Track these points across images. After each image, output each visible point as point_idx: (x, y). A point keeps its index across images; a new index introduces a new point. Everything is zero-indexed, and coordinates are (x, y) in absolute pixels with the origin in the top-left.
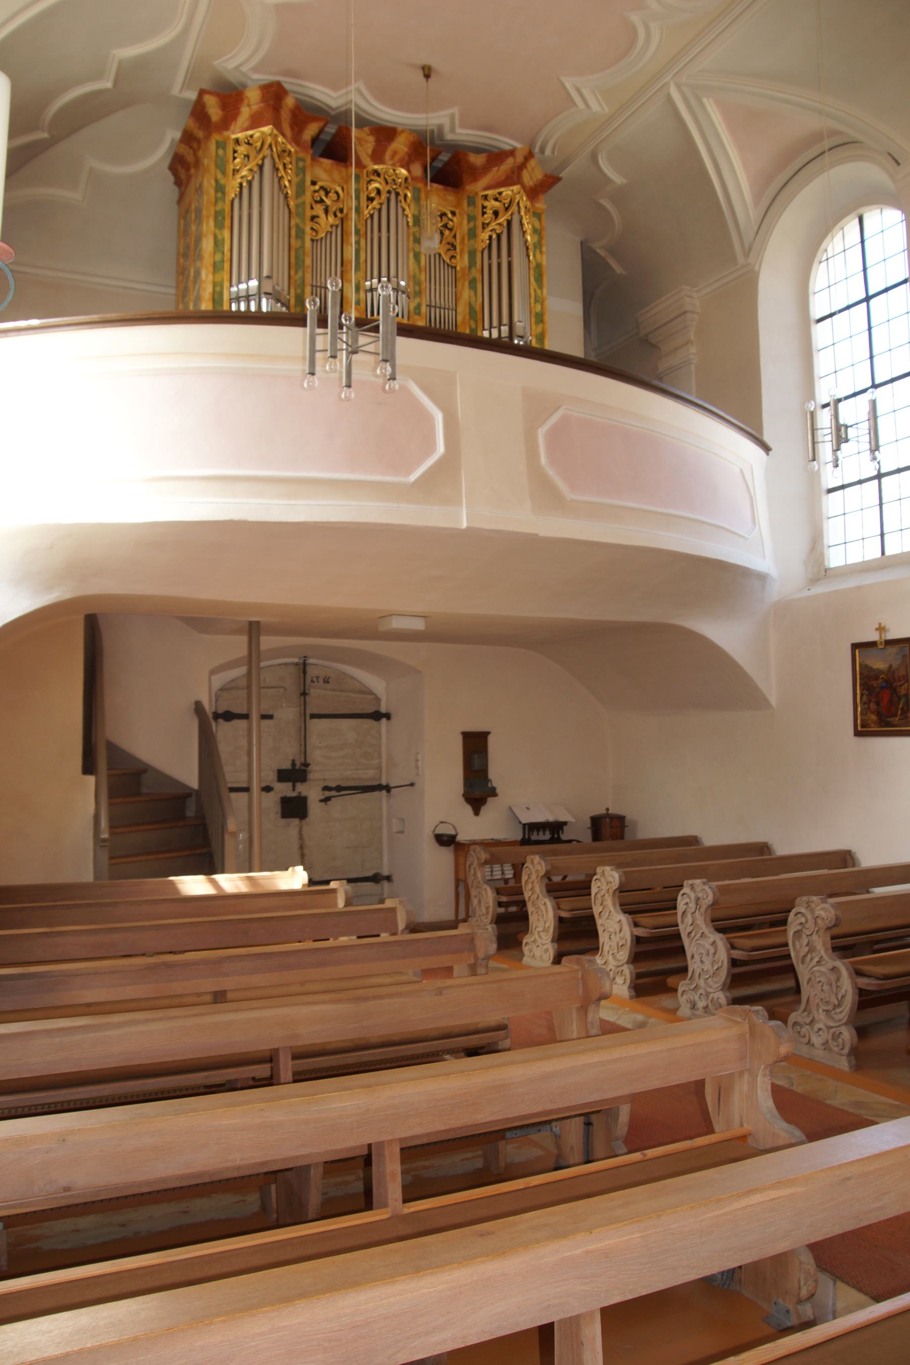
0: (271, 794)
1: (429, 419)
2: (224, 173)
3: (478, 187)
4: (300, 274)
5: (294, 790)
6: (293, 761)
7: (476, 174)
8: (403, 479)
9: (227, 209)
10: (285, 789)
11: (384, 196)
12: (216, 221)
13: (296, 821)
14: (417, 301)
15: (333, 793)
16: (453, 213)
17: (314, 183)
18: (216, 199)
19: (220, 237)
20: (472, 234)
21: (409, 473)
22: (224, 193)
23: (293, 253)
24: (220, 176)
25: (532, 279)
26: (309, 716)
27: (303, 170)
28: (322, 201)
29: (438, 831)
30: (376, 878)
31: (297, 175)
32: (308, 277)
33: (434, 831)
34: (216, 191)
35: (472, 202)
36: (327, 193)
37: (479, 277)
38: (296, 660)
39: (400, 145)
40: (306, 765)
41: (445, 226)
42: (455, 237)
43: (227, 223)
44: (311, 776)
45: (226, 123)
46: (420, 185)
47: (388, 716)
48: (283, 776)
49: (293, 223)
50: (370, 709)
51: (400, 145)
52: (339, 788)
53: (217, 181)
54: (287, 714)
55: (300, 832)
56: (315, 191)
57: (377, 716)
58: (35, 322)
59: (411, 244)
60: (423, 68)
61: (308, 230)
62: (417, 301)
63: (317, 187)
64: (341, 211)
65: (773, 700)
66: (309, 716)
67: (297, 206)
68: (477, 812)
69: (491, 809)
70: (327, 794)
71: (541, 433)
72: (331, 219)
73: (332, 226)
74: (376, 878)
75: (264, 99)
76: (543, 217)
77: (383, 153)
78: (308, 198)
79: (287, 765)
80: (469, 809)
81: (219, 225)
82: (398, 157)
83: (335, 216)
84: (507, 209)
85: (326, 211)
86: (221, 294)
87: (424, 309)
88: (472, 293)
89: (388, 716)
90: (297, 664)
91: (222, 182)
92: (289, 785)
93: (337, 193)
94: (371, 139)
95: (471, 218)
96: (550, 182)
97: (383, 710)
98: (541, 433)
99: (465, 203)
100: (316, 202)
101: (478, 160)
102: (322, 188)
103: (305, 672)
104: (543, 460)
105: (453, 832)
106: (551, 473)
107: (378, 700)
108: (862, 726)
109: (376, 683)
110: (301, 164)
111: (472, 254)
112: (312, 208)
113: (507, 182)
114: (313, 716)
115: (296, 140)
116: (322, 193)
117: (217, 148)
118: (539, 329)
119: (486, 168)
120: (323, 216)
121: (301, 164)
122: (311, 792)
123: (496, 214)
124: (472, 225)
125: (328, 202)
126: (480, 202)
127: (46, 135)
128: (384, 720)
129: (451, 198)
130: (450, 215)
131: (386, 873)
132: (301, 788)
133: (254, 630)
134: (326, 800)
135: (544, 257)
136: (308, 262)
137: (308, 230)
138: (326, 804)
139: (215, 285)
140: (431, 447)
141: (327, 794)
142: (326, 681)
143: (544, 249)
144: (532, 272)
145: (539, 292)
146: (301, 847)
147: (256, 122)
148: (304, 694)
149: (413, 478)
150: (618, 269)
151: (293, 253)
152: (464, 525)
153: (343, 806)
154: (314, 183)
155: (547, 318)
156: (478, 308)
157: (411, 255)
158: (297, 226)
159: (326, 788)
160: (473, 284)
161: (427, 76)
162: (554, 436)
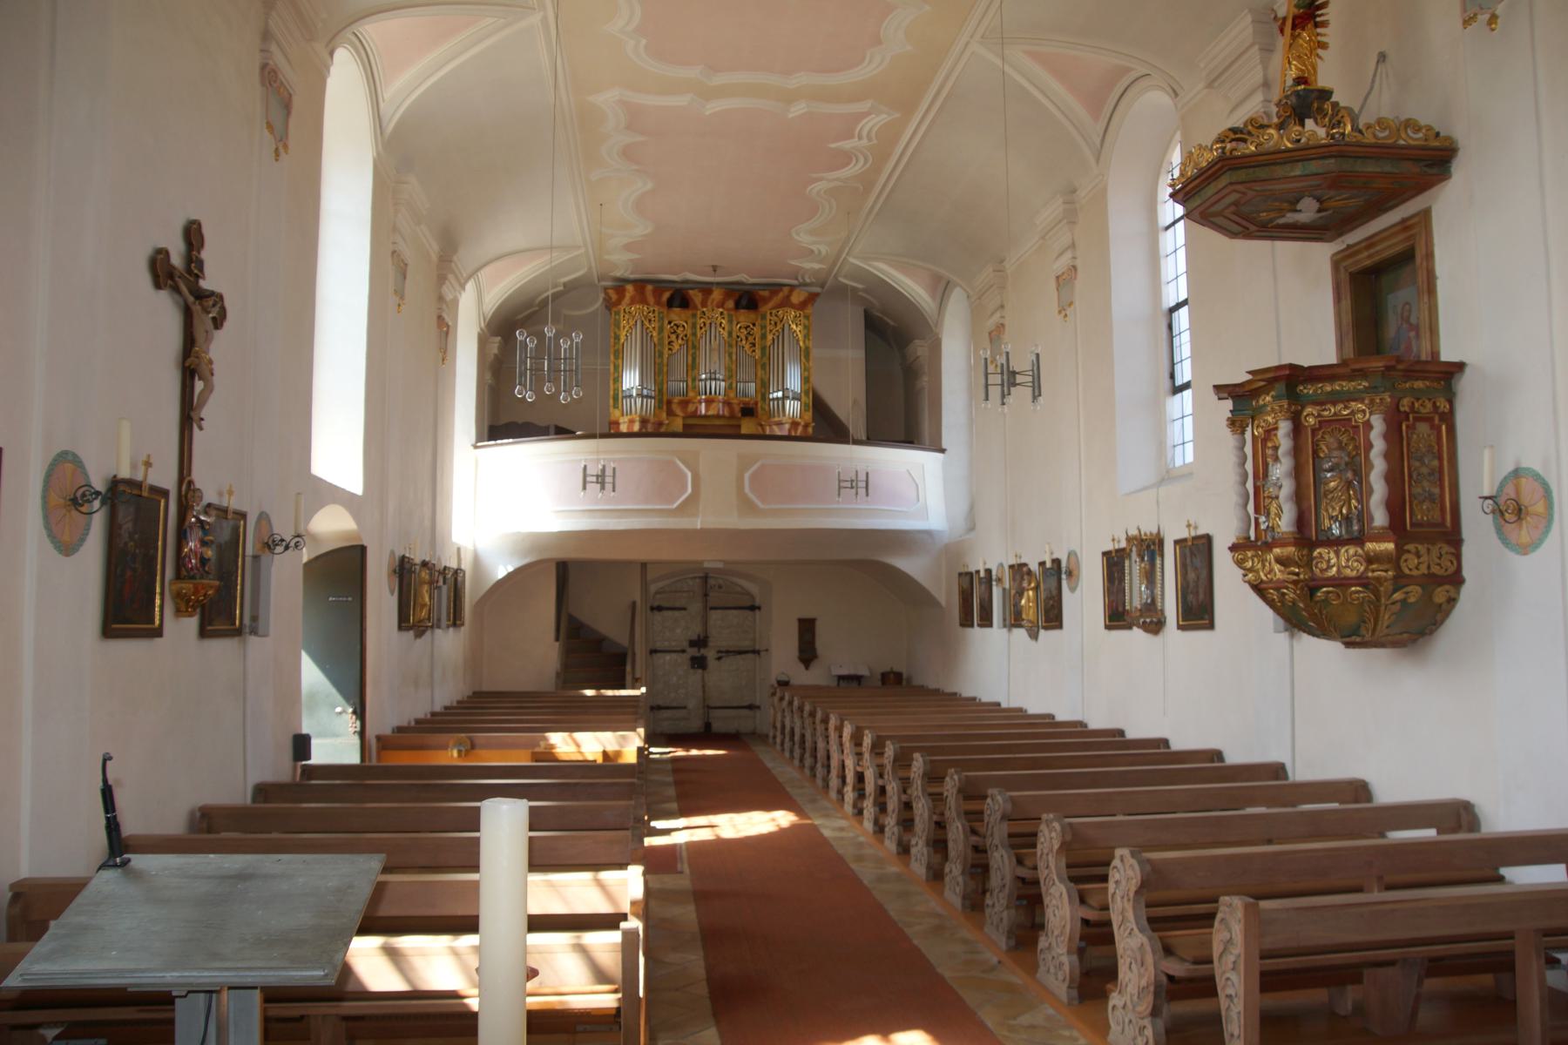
0: (685, 654)
1: (685, 476)
2: (619, 328)
3: (765, 309)
4: (661, 378)
5: (699, 651)
6: (699, 636)
7: (766, 300)
8: (670, 507)
9: (621, 348)
10: (693, 652)
11: (708, 325)
12: (615, 355)
13: (700, 671)
14: (730, 381)
15: (723, 654)
16: (754, 325)
17: (670, 323)
18: (615, 343)
19: (617, 363)
20: (764, 337)
21: (674, 503)
22: (619, 340)
23: (657, 366)
24: (617, 330)
25: (802, 358)
26: (708, 608)
27: (662, 319)
28: (675, 332)
29: (779, 679)
30: (751, 707)
31: (659, 321)
32: (665, 377)
33: (776, 679)
34: (615, 339)
35: (764, 317)
36: (678, 327)
37: (767, 362)
38: (701, 575)
39: (717, 295)
40: (706, 637)
41: (749, 333)
42: (755, 339)
43: (621, 356)
44: (711, 644)
45: (619, 302)
46: (732, 313)
47: (759, 608)
48: (693, 644)
49: (657, 349)
50: (749, 604)
51: (717, 295)
52: (727, 652)
53: (615, 333)
54: (695, 607)
55: (703, 677)
56: (671, 327)
57: (753, 608)
58: (511, 440)
59: (727, 348)
60: (713, 266)
61: (666, 351)
62: (730, 381)
63: (672, 324)
64: (686, 336)
65: (943, 603)
66: (708, 608)
67: (659, 339)
68: (807, 668)
69: (815, 666)
70: (720, 655)
71: (747, 476)
72: (680, 341)
73: (680, 346)
74: (751, 707)
75: (636, 290)
76: (811, 318)
77: (706, 302)
78: (666, 334)
79: (695, 637)
80: (802, 667)
81: (616, 357)
82: (715, 303)
83: (682, 339)
84: (781, 321)
85: (677, 337)
86: (618, 394)
87: (734, 385)
88: (763, 372)
89: (759, 608)
90: (700, 577)
91: (618, 333)
92: (695, 649)
93: (683, 326)
94: (700, 294)
95: (763, 327)
96: (813, 297)
97: (757, 604)
98: (747, 476)
99: (759, 320)
100: (672, 333)
101: (766, 293)
102: (675, 325)
103: (706, 582)
104: (747, 490)
105: (786, 679)
106: (752, 496)
107: (753, 598)
108: (1015, 620)
109: (753, 588)
110: (661, 315)
111: (763, 349)
112: (669, 337)
113: (781, 305)
114: (711, 608)
115: (658, 303)
116: (675, 327)
117: (615, 315)
118: (807, 387)
119: (770, 298)
120: (675, 341)
121: (661, 315)
122: (710, 654)
123: (776, 323)
124: (763, 331)
125: (679, 331)
126: (768, 317)
127: (537, 308)
128: (757, 611)
129: (752, 316)
130: (751, 326)
131: (758, 703)
132: (703, 651)
133: (644, 565)
134: (719, 658)
135: (811, 342)
136: (665, 369)
137: (666, 351)
138: (892, 668)
139: (614, 390)
140: (684, 488)
141: (720, 655)
142: (720, 587)
143: (811, 338)
144: (802, 353)
145: (807, 365)
146: (704, 687)
147: (632, 302)
148: (706, 595)
149: (675, 505)
150: (892, 323)
151: (657, 366)
152: (699, 527)
153: (731, 663)
154: (670, 323)
155: (811, 379)
156: (766, 380)
157: (727, 355)
158: (659, 351)
159: (719, 652)
160: (763, 367)
161: (715, 271)
162: (753, 478)
